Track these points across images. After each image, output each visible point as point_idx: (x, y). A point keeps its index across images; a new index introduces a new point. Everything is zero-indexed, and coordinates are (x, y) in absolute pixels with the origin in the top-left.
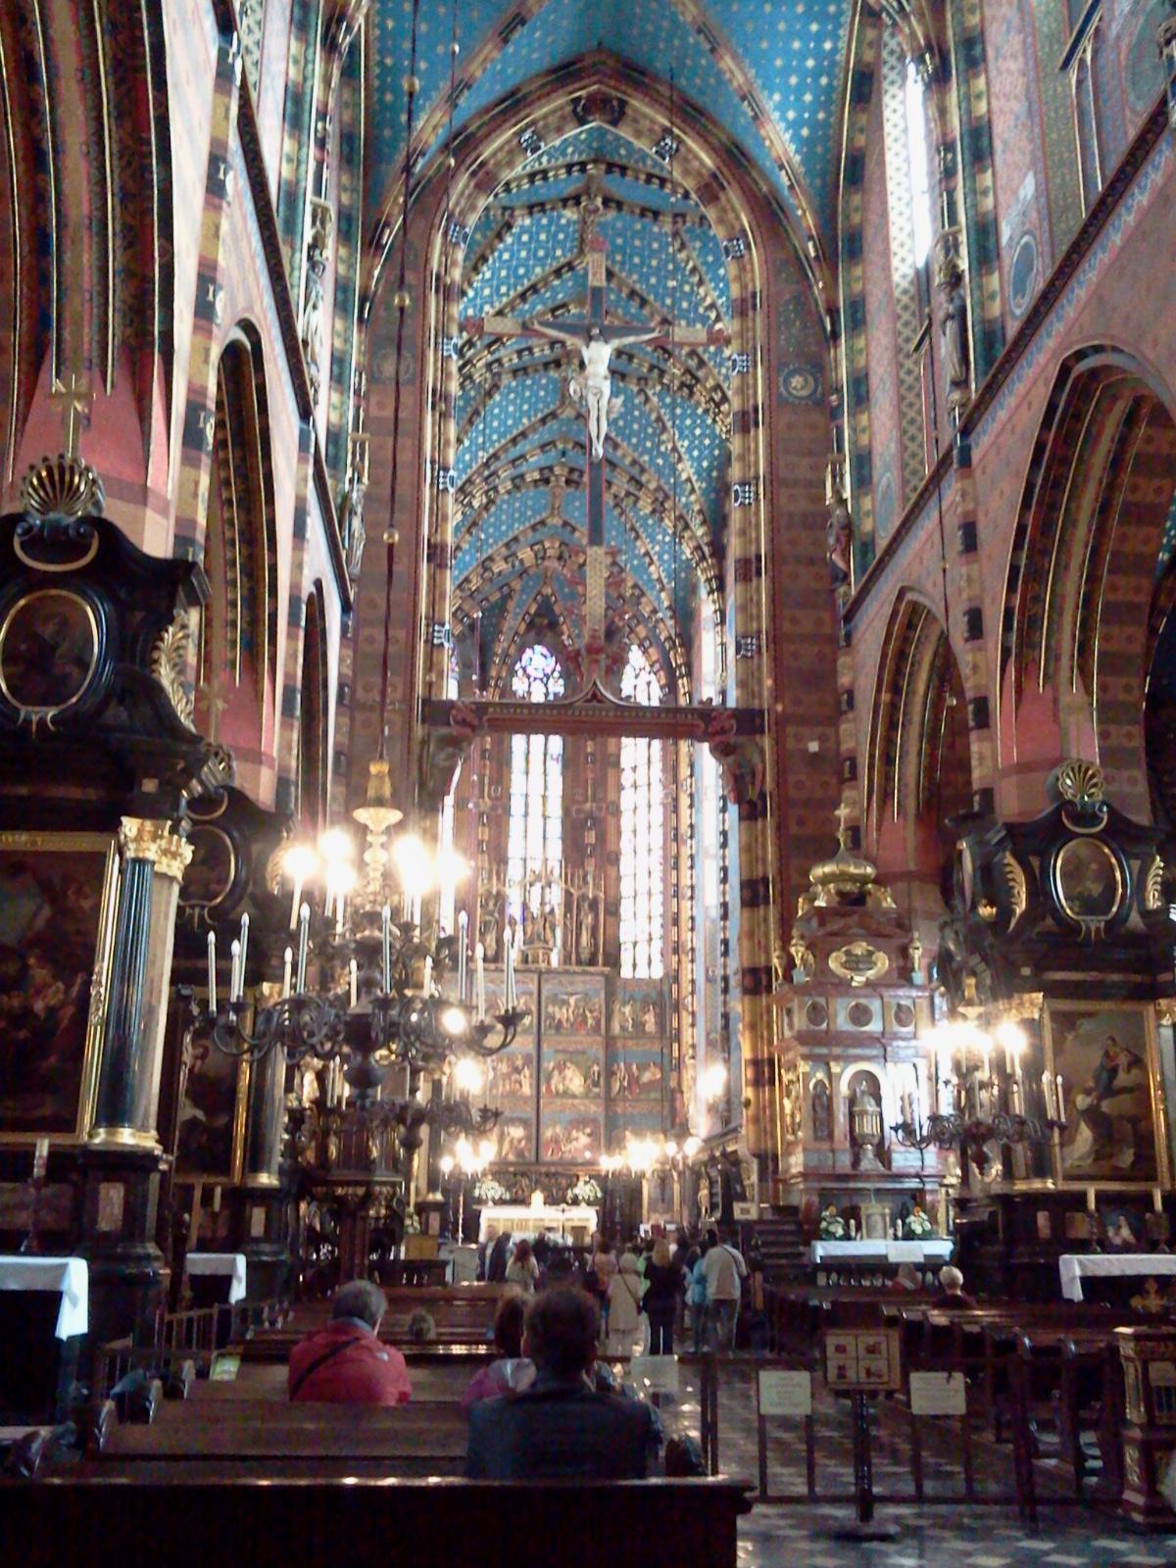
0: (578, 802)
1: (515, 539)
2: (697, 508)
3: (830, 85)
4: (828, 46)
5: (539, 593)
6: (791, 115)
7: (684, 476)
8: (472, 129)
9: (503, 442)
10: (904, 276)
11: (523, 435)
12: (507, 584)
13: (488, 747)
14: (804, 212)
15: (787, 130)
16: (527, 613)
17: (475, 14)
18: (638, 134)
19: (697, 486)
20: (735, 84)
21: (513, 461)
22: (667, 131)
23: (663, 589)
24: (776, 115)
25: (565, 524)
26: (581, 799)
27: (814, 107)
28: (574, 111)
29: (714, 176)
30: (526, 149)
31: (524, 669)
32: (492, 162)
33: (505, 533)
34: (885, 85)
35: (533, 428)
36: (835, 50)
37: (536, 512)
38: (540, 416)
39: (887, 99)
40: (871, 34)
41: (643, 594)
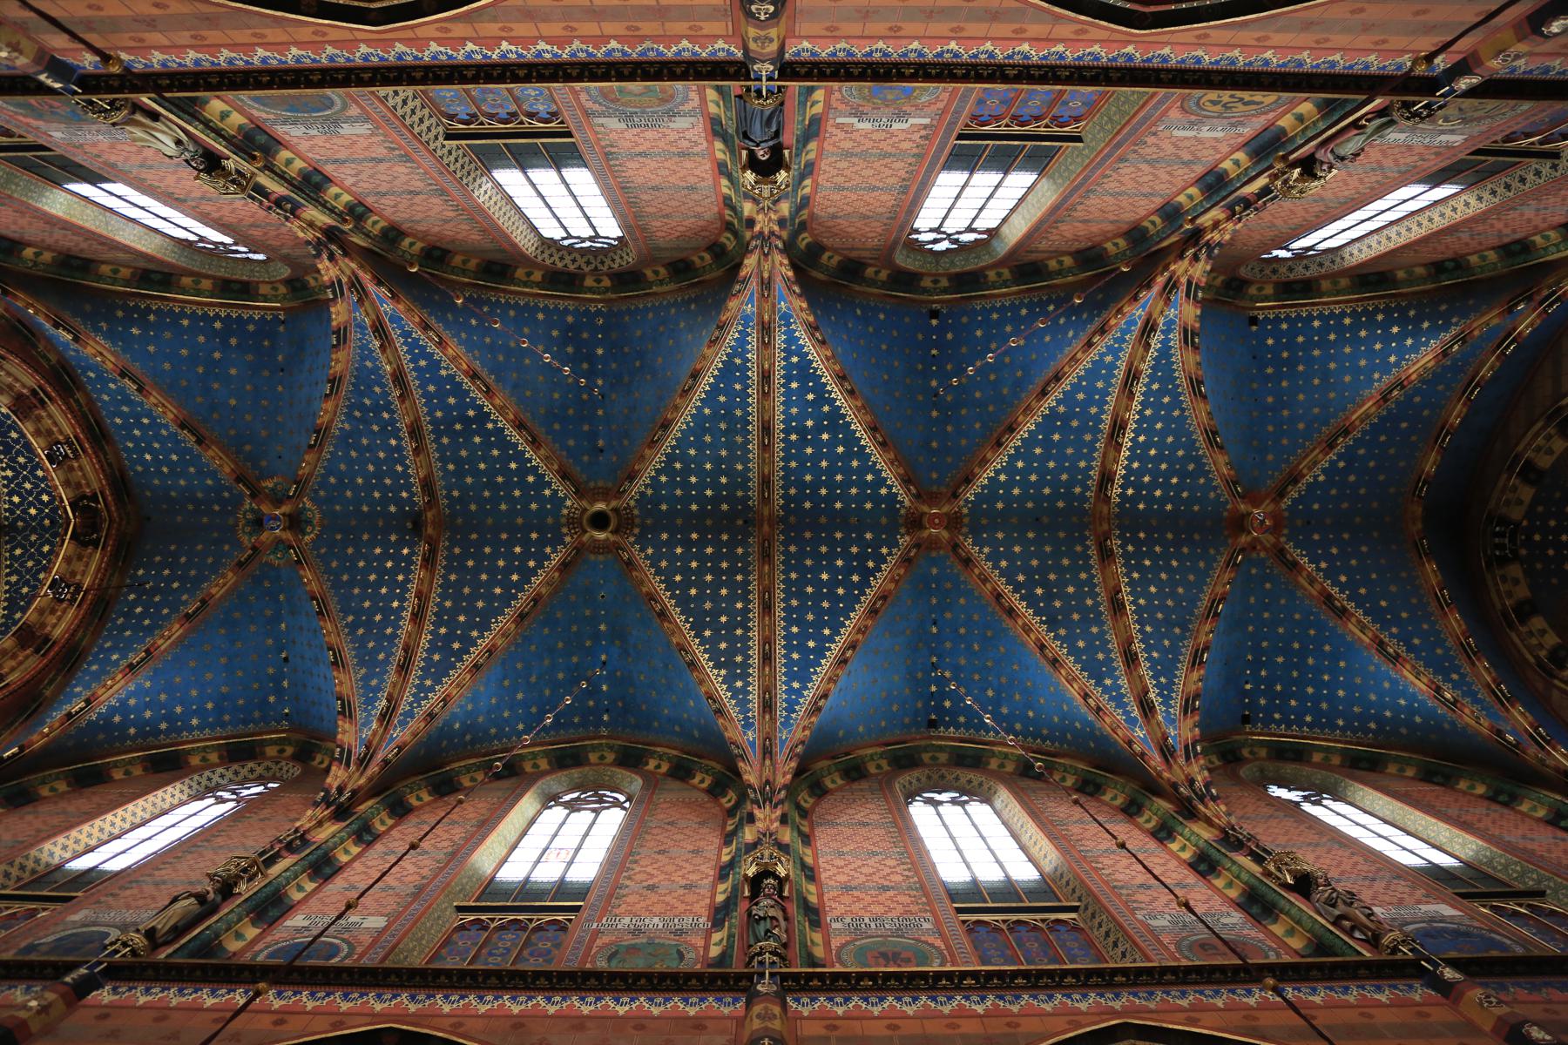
3: (161, 732)
4: (195, 722)
6: (132, 702)
8: (78, 395)
10: (52, 854)
14: (47, 735)
15: (119, 700)
17: (199, 400)
18: (67, 560)
20: (160, 642)
22: (79, 587)
24: (132, 687)
27: (140, 724)
28: (84, 497)
29: (47, 639)
30: (51, 449)
32: (44, 414)
34: (187, 781)
36: (191, 729)
39: (178, 785)
40: (214, 757)
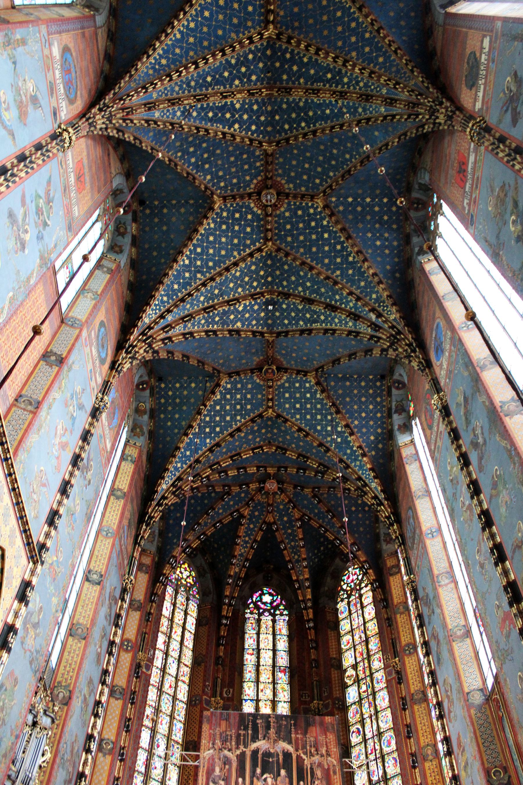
0: (305, 703)
1: (239, 430)
2: (385, 294)
5: (264, 522)
7: (371, 271)
9: (218, 269)
11: (236, 264)
12: (237, 511)
13: (221, 654)
16: (255, 541)
19: (385, 281)
21: (228, 302)
23: (364, 455)
25: (278, 416)
26: (308, 699)
31: (255, 604)
33: (229, 424)
35: (243, 259)
37: (255, 407)
38: (248, 251)
41: (348, 467)
